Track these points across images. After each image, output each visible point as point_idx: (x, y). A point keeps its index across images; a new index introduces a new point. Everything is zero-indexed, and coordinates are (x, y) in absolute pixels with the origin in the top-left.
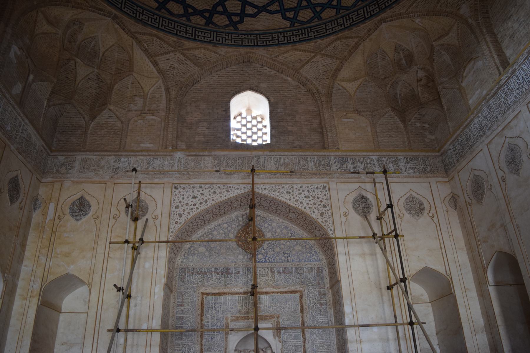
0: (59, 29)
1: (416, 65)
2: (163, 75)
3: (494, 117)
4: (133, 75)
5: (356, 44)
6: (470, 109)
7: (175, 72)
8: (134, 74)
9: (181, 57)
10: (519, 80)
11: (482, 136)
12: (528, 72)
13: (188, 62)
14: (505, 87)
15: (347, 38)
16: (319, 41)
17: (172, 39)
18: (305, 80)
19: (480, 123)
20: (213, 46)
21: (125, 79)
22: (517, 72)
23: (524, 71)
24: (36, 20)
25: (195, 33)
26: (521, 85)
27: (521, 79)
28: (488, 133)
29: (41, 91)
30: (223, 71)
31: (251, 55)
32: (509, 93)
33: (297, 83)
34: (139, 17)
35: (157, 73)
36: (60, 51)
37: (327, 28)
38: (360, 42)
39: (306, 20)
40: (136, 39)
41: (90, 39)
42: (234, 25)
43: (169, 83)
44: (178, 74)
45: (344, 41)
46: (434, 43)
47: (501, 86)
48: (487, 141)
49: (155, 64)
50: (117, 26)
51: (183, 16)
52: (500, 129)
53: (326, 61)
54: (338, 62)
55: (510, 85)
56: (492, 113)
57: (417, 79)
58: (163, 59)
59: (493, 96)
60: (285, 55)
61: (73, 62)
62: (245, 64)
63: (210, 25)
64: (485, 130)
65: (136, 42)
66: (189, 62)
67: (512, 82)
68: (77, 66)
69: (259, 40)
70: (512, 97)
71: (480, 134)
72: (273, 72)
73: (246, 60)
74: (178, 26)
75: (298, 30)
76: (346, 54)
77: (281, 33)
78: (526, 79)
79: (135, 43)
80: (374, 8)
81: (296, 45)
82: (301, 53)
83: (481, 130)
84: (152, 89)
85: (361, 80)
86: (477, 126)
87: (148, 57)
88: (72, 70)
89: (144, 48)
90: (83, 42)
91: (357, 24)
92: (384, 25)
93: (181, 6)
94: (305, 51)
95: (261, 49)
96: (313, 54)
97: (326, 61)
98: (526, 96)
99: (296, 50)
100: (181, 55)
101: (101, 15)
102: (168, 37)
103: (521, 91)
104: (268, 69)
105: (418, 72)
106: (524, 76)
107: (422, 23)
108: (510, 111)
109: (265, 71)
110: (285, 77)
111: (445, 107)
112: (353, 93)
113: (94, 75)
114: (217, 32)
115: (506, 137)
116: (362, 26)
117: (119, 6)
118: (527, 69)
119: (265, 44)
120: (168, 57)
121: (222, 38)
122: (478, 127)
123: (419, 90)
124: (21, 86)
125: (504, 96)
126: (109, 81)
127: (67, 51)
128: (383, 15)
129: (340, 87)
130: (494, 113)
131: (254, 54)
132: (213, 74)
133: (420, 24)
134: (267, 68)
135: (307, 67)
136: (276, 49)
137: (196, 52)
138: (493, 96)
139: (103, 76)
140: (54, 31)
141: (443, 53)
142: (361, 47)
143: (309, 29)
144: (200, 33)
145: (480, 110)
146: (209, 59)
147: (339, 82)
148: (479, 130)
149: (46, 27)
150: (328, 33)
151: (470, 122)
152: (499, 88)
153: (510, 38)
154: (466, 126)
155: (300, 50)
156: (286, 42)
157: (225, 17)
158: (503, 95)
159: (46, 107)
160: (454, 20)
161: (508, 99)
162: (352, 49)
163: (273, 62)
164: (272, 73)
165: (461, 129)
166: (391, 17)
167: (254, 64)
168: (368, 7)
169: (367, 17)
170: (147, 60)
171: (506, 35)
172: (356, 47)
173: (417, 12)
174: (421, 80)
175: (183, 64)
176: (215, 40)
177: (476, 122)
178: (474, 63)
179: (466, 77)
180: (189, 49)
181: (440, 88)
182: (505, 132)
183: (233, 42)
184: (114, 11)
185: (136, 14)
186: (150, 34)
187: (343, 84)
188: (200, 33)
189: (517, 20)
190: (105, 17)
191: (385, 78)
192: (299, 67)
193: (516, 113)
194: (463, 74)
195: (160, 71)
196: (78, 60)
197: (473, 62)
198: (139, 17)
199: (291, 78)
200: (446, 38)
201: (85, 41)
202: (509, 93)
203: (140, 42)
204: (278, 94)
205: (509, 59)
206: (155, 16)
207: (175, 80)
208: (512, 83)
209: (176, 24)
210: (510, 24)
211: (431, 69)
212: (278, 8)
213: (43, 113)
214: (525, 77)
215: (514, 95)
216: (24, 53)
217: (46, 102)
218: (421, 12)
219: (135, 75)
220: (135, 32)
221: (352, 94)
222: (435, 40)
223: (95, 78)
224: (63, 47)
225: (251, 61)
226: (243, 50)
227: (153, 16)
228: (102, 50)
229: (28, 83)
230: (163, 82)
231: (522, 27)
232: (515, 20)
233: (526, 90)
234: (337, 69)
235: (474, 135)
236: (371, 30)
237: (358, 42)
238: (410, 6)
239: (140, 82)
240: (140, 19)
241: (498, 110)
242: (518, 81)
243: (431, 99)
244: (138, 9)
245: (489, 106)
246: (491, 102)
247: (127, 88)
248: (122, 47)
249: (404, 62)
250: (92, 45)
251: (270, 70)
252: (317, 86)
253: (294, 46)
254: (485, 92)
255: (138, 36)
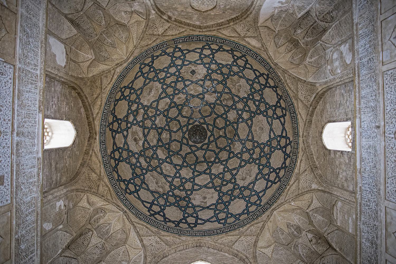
0: (92, 207)
1: (304, 230)
2: (145, 248)
3: (373, 227)
4: (125, 246)
5: (263, 225)
6: (353, 235)
7: (153, 248)
8: (126, 245)
9: (158, 240)
10: (368, 191)
11: (376, 249)
12: (369, 182)
13: (162, 243)
14: (363, 202)
15: (257, 223)
16: (241, 229)
17: (154, 229)
18: (237, 252)
19: (367, 239)
20: (178, 236)
21: (119, 248)
22: (363, 188)
23: (366, 184)
24: (82, 198)
25: (168, 229)
26: (371, 192)
27: (368, 189)
28: (379, 242)
29: (61, 240)
30: (183, 251)
31: (201, 241)
32: (368, 203)
33: (232, 256)
34: (139, 215)
35: (141, 247)
36: (87, 220)
37: (244, 222)
38: (265, 224)
39: (231, 222)
40: (134, 225)
41: (107, 224)
42: (192, 228)
43: (148, 253)
44: (155, 250)
45: (256, 226)
46: (307, 211)
47: (360, 203)
48: (383, 249)
49: (141, 241)
50: (125, 217)
51: (163, 221)
52: (384, 231)
53: (248, 239)
54: (255, 237)
55: (365, 198)
56: (370, 225)
57: (309, 240)
58: (147, 239)
59: (361, 214)
60: (222, 239)
61: (91, 233)
62: (197, 248)
63: (178, 227)
64: (375, 241)
65: (133, 227)
66: (163, 243)
67: (365, 195)
68: (93, 236)
69: (205, 233)
70: (372, 204)
71: (374, 248)
72: (216, 251)
73: (198, 245)
74: (159, 225)
75: (228, 227)
76: (258, 231)
77: (218, 229)
78: (371, 187)
79: (132, 227)
80: (267, 206)
81: (228, 233)
82: (231, 237)
83: (372, 244)
84: (136, 257)
85: (273, 246)
86: (368, 244)
87: (138, 237)
88: (88, 239)
89: (137, 231)
90: (102, 225)
91: (260, 216)
92: (275, 212)
93: (163, 218)
94: (234, 235)
95: (207, 237)
96: (239, 236)
97: (248, 239)
98: (380, 194)
99: (229, 236)
100: (158, 239)
101: (118, 209)
102: (152, 228)
103: (375, 195)
104: (212, 250)
105: (307, 235)
106: (368, 186)
107: (296, 204)
108: (379, 212)
109: (210, 251)
110: (223, 254)
111: (338, 249)
112: (271, 256)
113: (100, 244)
114: (181, 230)
115: (393, 233)
116: (263, 216)
117: (129, 208)
118: (367, 181)
119: (209, 234)
120: (150, 239)
121: (184, 233)
122: (368, 244)
123: (314, 247)
124: (51, 227)
125: (368, 207)
126: (108, 249)
127: (91, 224)
128: (273, 207)
129: (261, 253)
130: (371, 224)
131: (203, 240)
132: (177, 253)
133: (295, 205)
134: (211, 249)
135: (237, 244)
136: (216, 237)
137: (168, 238)
138: (361, 214)
139: (106, 245)
140: (89, 208)
141: (316, 215)
142: (266, 227)
143: (234, 225)
144: (171, 229)
145: (360, 229)
146: (175, 242)
147: (259, 249)
148: (371, 246)
149: (85, 204)
150: (245, 224)
151: (360, 244)
152: (360, 206)
153: (346, 181)
154: (360, 250)
155: (231, 236)
156: (222, 232)
157: (186, 224)
158: (366, 208)
159: (59, 254)
160: (312, 193)
161: (371, 207)
162: (261, 228)
163: (215, 244)
164: (215, 252)
165: (358, 256)
166: (278, 206)
167: (203, 247)
168: (264, 207)
169: (264, 211)
170: (137, 238)
171: (343, 182)
172: (263, 227)
173: (290, 199)
174: (312, 240)
175: (159, 244)
176: (180, 233)
177: (365, 242)
178: (336, 207)
179: (337, 219)
180: (163, 236)
181: (325, 235)
182: (389, 230)
183: (190, 234)
184: (125, 209)
185: (137, 214)
186: (143, 225)
187: (261, 250)
188: (171, 229)
189: (343, 171)
190: (120, 211)
191: (288, 244)
192: (231, 245)
193: (384, 211)
194: (334, 218)
195: (143, 246)
196: (94, 232)
197: (335, 207)
198: (139, 215)
199: (227, 253)
200: (312, 205)
201: (104, 225)
202: (368, 203)
203: (135, 227)
204: (220, 262)
205: (354, 190)
206: (147, 218)
207: (152, 252)
208: (365, 197)
209: (158, 223)
210: (341, 176)
211: (314, 229)
212: (216, 219)
213: (54, 257)
214: (369, 186)
215: (373, 201)
216: (65, 210)
217: (60, 251)
218: (293, 197)
219: (127, 246)
220: (134, 222)
221: (270, 256)
222: (308, 209)
223: (101, 247)
224: (90, 221)
225: (202, 245)
226: (196, 238)
227: (147, 217)
228: (112, 232)
229: (56, 228)
230: (144, 252)
231: (348, 171)
232: (342, 172)
233: (376, 192)
234: (256, 241)
235: (371, 253)
236: (269, 216)
237: (264, 224)
238: (285, 197)
239: (129, 251)
240: (139, 216)
241: (372, 220)
242: (368, 192)
243: (325, 249)
244: (139, 213)
245: (364, 223)
246: (362, 219)
247: (119, 255)
248: (124, 231)
249: (295, 233)
250: (107, 228)
251: (214, 250)
252: (245, 254)
253: (227, 234)
254: (354, 216)
255: (135, 224)
